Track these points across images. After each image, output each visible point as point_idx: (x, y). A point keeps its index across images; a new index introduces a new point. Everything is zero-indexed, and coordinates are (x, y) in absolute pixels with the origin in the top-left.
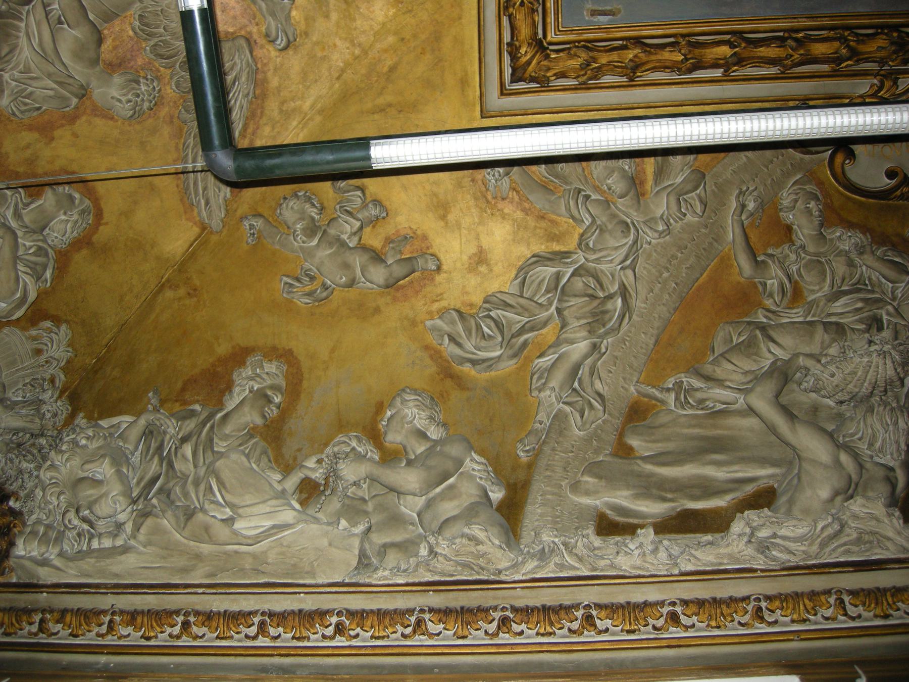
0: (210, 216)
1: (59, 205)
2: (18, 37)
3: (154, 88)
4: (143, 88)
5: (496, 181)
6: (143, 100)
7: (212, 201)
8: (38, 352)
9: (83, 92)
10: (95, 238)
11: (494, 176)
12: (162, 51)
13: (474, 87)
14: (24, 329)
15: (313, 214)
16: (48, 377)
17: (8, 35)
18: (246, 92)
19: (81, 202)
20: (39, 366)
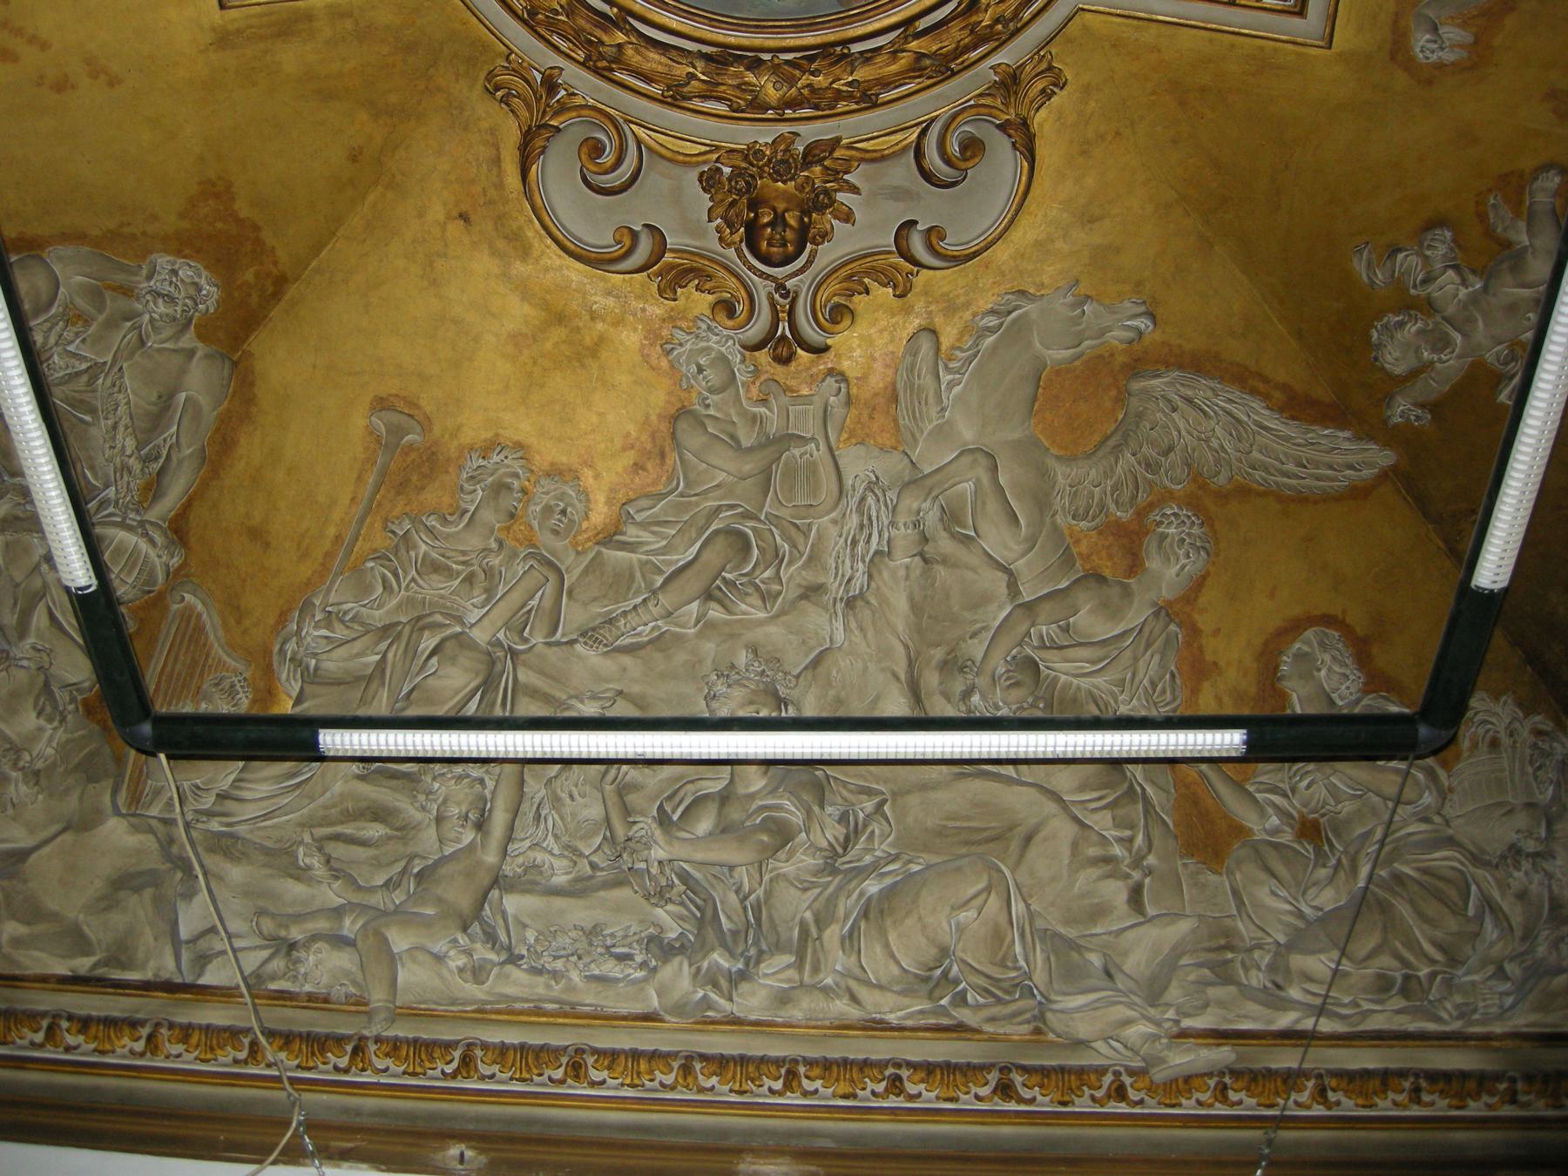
0: (1370, 465)
1: (1308, 676)
2: (1078, 688)
3: (1174, 514)
4: (1172, 530)
5: (1442, 49)
6: (1189, 534)
7: (1351, 458)
8: (1494, 744)
9: (1163, 613)
10: (1360, 631)
11: (1433, 52)
12: (1127, 494)
13: (1275, 50)
14: (1458, 757)
15: (1414, 329)
16: (1532, 739)
17: (1075, 700)
18: (1210, 394)
19: (1308, 643)
20: (1514, 747)
